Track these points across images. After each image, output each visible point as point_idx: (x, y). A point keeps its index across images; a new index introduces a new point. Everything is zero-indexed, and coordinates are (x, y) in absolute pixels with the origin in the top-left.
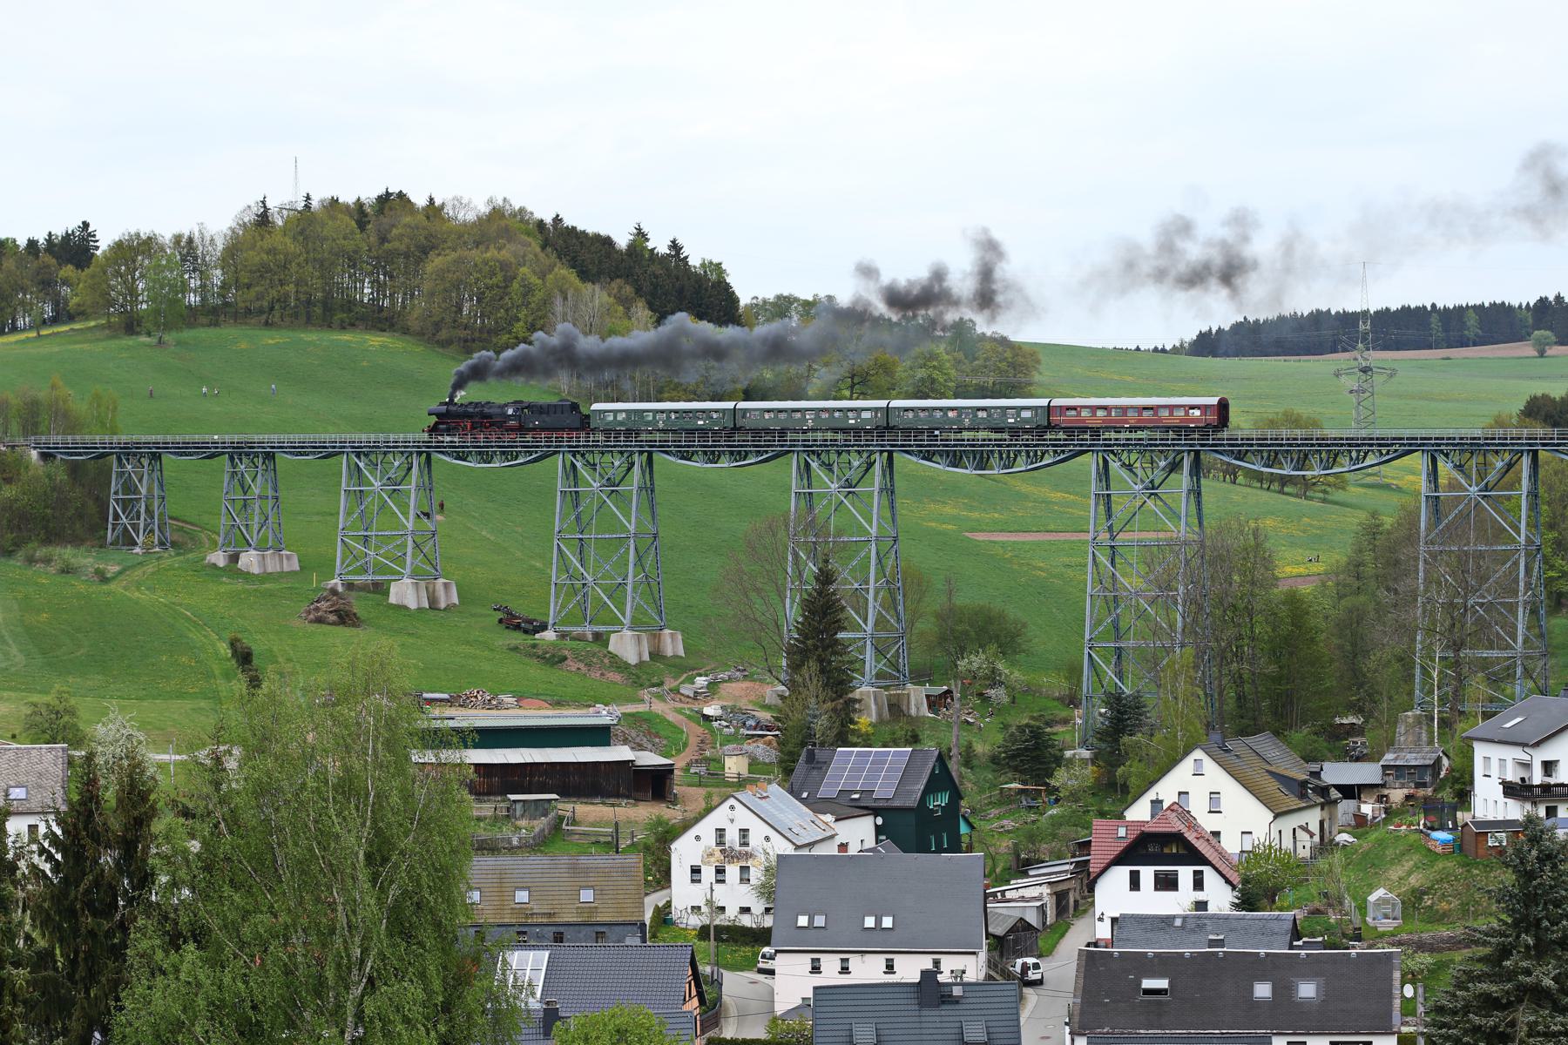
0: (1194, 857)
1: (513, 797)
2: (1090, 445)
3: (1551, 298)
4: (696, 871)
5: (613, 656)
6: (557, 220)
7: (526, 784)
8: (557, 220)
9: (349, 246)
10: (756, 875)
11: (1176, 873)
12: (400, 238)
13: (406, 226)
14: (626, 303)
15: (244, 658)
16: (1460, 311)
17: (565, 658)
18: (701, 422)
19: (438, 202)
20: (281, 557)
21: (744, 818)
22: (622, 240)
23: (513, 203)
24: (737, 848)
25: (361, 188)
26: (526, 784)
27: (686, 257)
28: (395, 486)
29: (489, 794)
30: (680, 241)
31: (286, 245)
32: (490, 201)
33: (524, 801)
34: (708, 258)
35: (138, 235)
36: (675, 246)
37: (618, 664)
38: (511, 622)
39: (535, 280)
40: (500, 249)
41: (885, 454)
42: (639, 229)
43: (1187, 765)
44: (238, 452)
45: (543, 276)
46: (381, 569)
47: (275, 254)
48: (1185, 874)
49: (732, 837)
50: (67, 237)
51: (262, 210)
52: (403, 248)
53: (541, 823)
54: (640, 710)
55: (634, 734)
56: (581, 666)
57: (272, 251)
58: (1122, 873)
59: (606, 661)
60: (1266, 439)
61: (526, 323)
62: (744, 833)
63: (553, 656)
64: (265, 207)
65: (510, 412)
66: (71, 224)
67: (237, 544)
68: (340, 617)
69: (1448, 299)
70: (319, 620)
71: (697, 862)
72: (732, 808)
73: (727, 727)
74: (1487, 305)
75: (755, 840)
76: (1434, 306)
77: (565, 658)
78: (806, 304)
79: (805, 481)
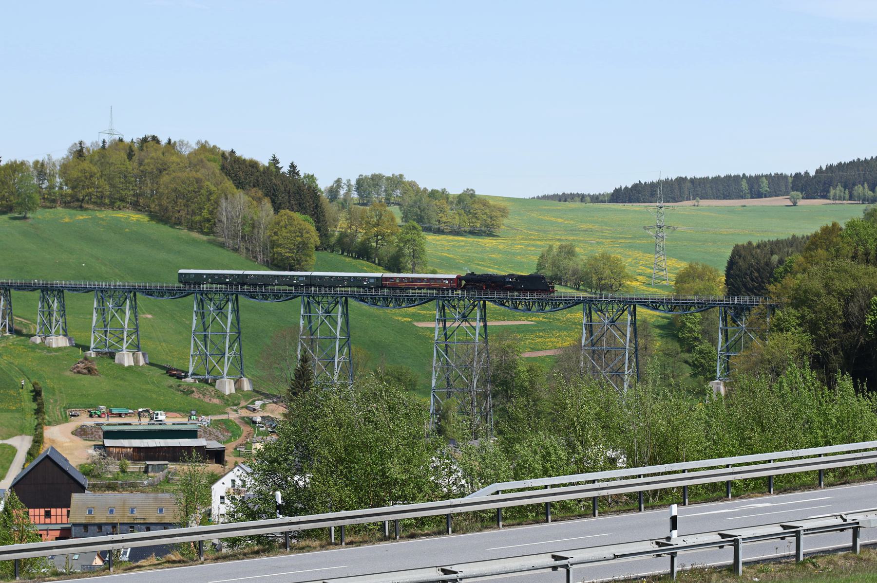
1: (148, 463)
2: (435, 297)
3: (803, 173)
4: (222, 498)
5: (217, 391)
7: (157, 456)
8: (233, 152)
9: (123, 168)
12: (148, 164)
13: (152, 158)
14: (259, 200)
15: (37, 394)
16: (758, 178)
17: (193, 392)
19: (172, 141)
23: (210, 143)
25: (132, 134)
26: (157, 456)
27: (298, 171)
28: (120, 307)
29: (140, 460)
30: (295, 164)
31: (90, 168)
32: (198, 143)
33: (153, 465)
34: (307, 173)
35: (15, 162)
36: (293, 166)
37: (220, 396)
38: (170, 372)
39: (213, 188)
40: (197, 171)
41: (344, 298)
42: (274, 157)
44: (47, 290)
45: (216, 185)
47: (85, 173)
49: (238, 482)
51: (79, 148)
52: (149, 169)
53: (160, 475)
54: (223, 418)
55: (214, 431)
56: (201, 395)
57: (84, 171)
59: (213, 393)
61: (208, 210)
63: (188, 391)
64: (81, 146)
67: (46, 334)
68: (89, 371)
69: (751, 172)
70: (79, 372)
71: (223, 495)
72: (238, 470)
73: (262, 427)
74: (773, 174)
76: (744, 175)
77: (193, 392)
78: (388, 179)
79: (308, 310)
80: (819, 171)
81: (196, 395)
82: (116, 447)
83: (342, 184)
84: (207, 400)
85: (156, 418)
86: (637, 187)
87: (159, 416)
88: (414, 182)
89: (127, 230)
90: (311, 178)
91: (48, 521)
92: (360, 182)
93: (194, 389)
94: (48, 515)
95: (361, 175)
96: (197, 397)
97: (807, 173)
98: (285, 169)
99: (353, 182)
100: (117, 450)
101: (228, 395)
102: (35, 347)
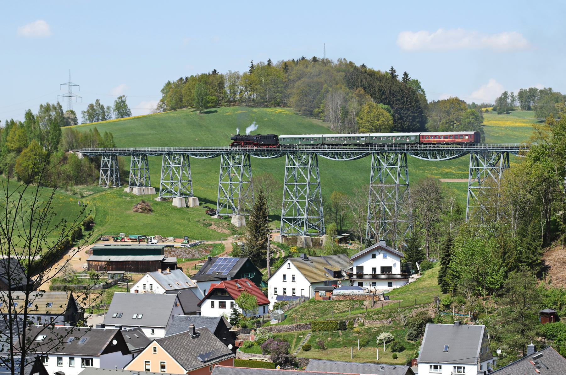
0: (230, 297)
6: (363, 66)
11: (225, 302)
17: (211, 225)
18: (312, 142)
20: (148, 189)
21: (152, 281)
24: (149, 291)
36: (406, 75)
42: (392, 69)
43: (286, 265)
48: (228, 302)
49: (148, 287)
56: (216, 227)
58: (209, 302)
60: (514, 147)
65: (255, 138)
70: (137, 211)
78: (541, 91)
81: (213, 227)
82: (94, 261)
83: (508, 96)
84: (219, 231)
85: (150, 241)
87: (153, 240)
88: (560, 93)
89: (266, 119)
90: (416, 82)
92: (522, 94)
93: (212, 223)
95: (522, 89)
96: (213, 228)
98: (400, 78)
99: (516, 94)
100: (95, 263)
101: (239, 228)
102: (127, 195)
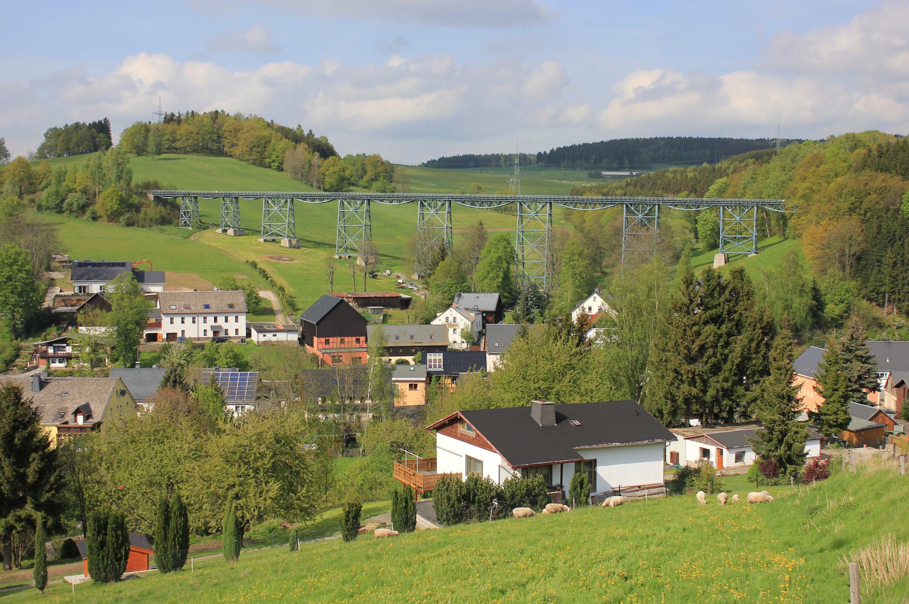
10: (459, 331)
16: (510, 155)
22: (295, 128)
43: (592, 298)
44: (225, 197)
46: (277, 235)
49: (451, 319)
50: (100, 122)
62: (455, 318)
66: (102, 119)
69: (506, 152)
75: (458, 321)
80: (552, 151)
86: (442, 160)
91: (342, 346)
94: (342, 341)
97: (545, 152)
98: (306, 133)
